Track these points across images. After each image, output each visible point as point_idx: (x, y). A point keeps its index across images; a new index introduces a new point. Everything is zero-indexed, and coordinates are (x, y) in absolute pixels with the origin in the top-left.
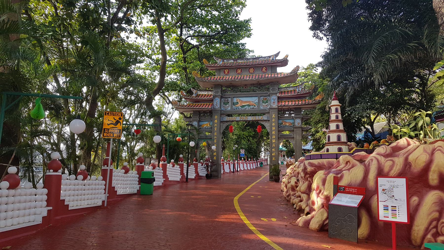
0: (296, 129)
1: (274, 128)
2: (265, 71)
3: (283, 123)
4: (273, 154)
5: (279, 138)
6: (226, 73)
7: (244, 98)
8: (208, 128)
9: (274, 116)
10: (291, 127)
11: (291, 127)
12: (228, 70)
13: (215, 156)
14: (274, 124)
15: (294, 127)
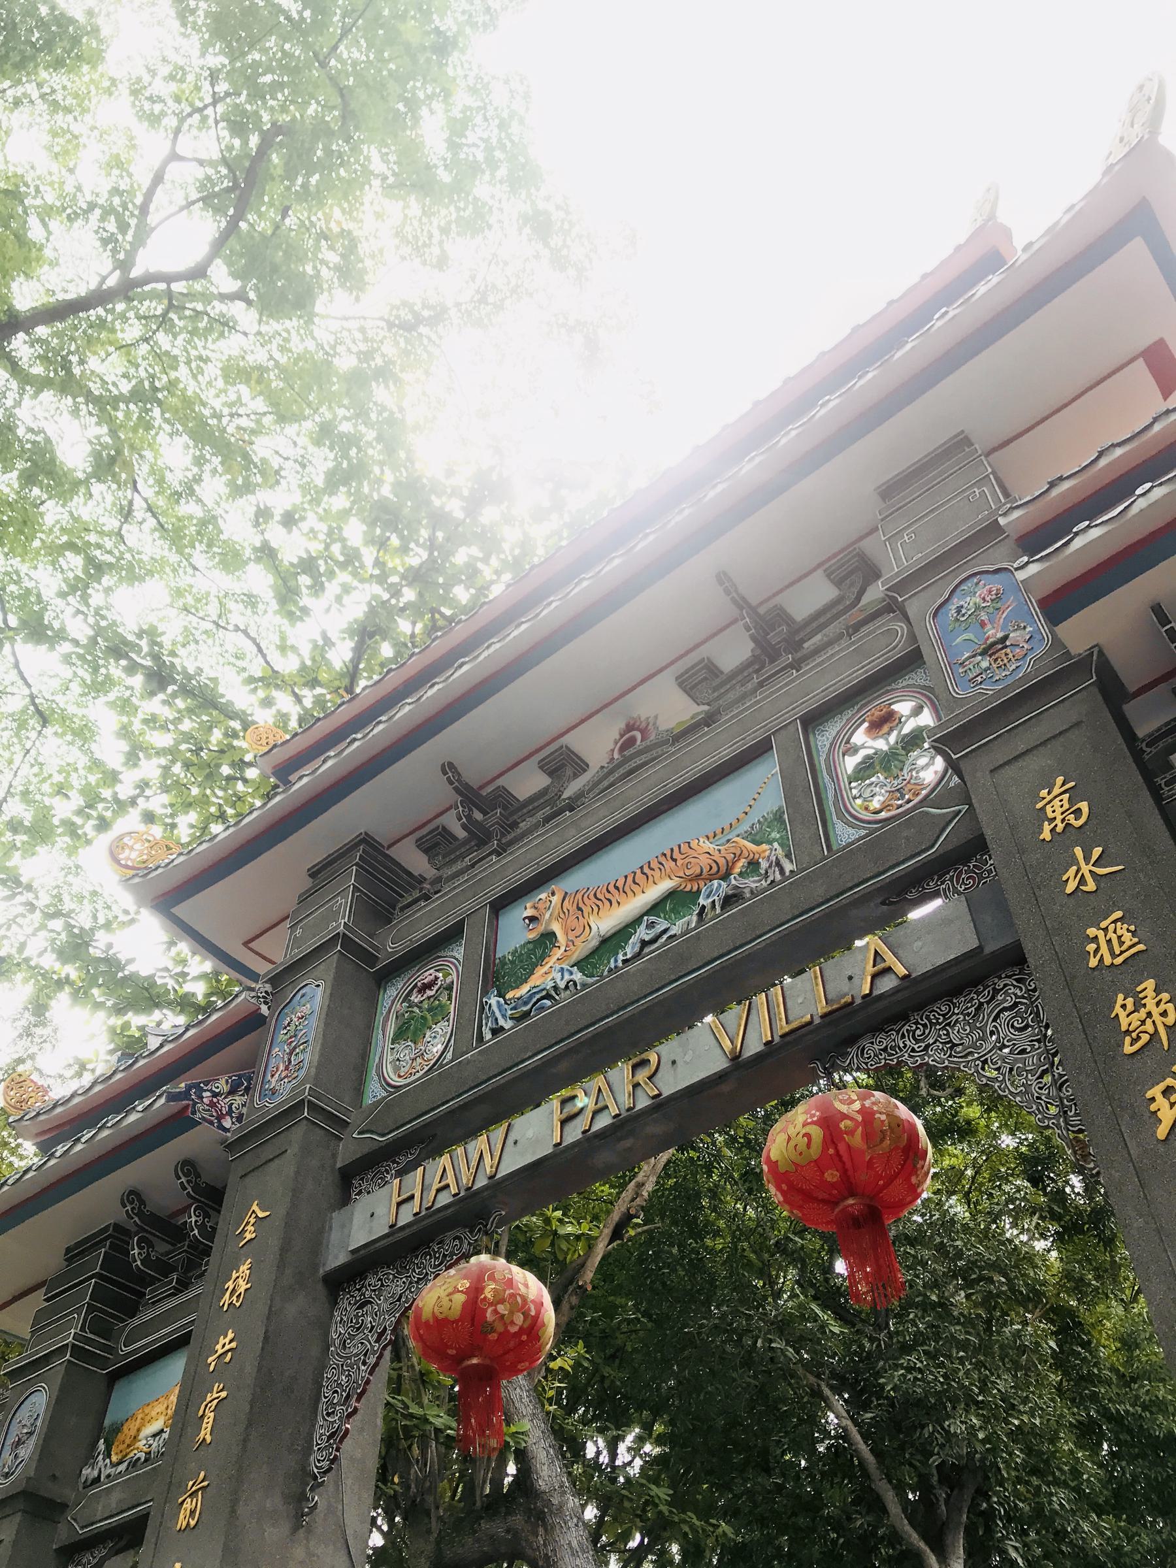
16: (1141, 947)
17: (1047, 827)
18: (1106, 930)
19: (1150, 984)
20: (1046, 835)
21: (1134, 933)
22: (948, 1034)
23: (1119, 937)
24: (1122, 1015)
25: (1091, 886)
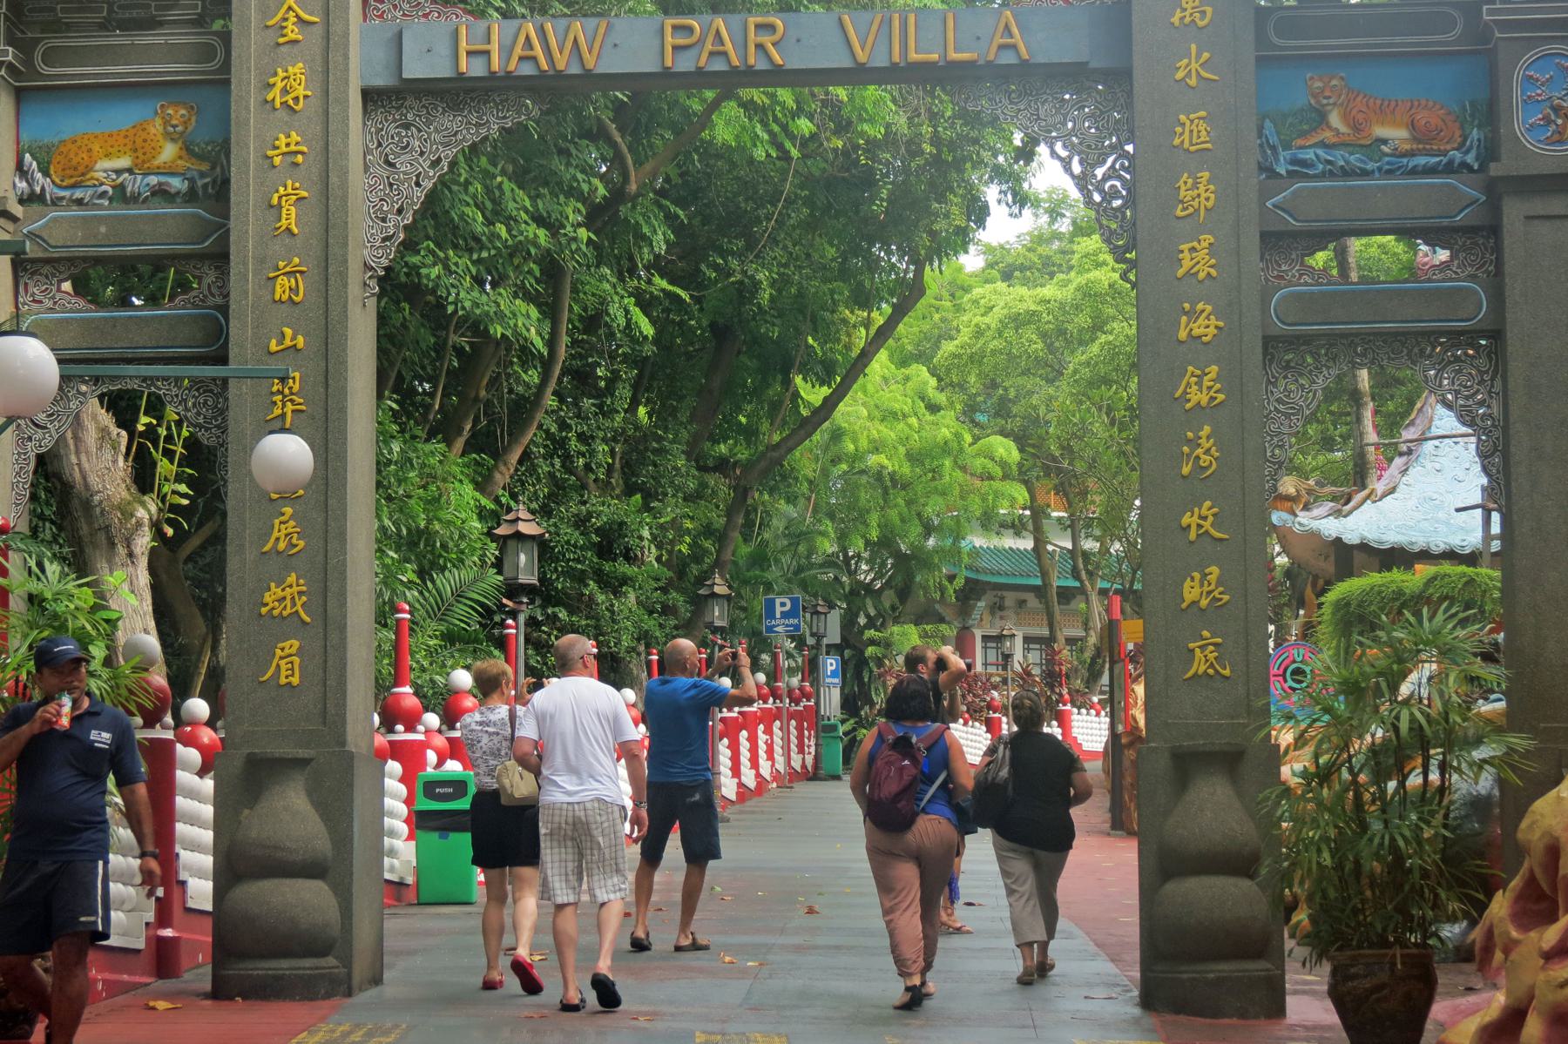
0: (1539, 206)
3: (1335, 119)
4: (1191, 591)
5: (1272, 345)
8: (161, 193)
10: (1449, 169)
11: (1449, 169)
13: (288, 625)
15: (1495, 170)
16: (1208, 146)
17: (1178, 14)
18: (1192, 121)
19: (1206, 175)
20: (1176, 20)
21: (1208, 133)
22: (1038, 110)
23: (1199, 132)
24: (1183, 188)
25: (1193, 82)
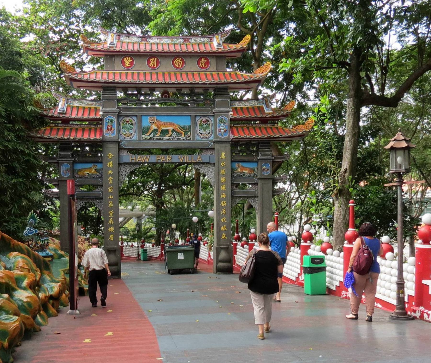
1: (223, 180)
2: (205, 66)
4: (222, 228)
6: (127, 64)
7: (166, 117)
9: (223, 156)
12: (131, 59)
13: (111, 233)
14: (223, 172)
